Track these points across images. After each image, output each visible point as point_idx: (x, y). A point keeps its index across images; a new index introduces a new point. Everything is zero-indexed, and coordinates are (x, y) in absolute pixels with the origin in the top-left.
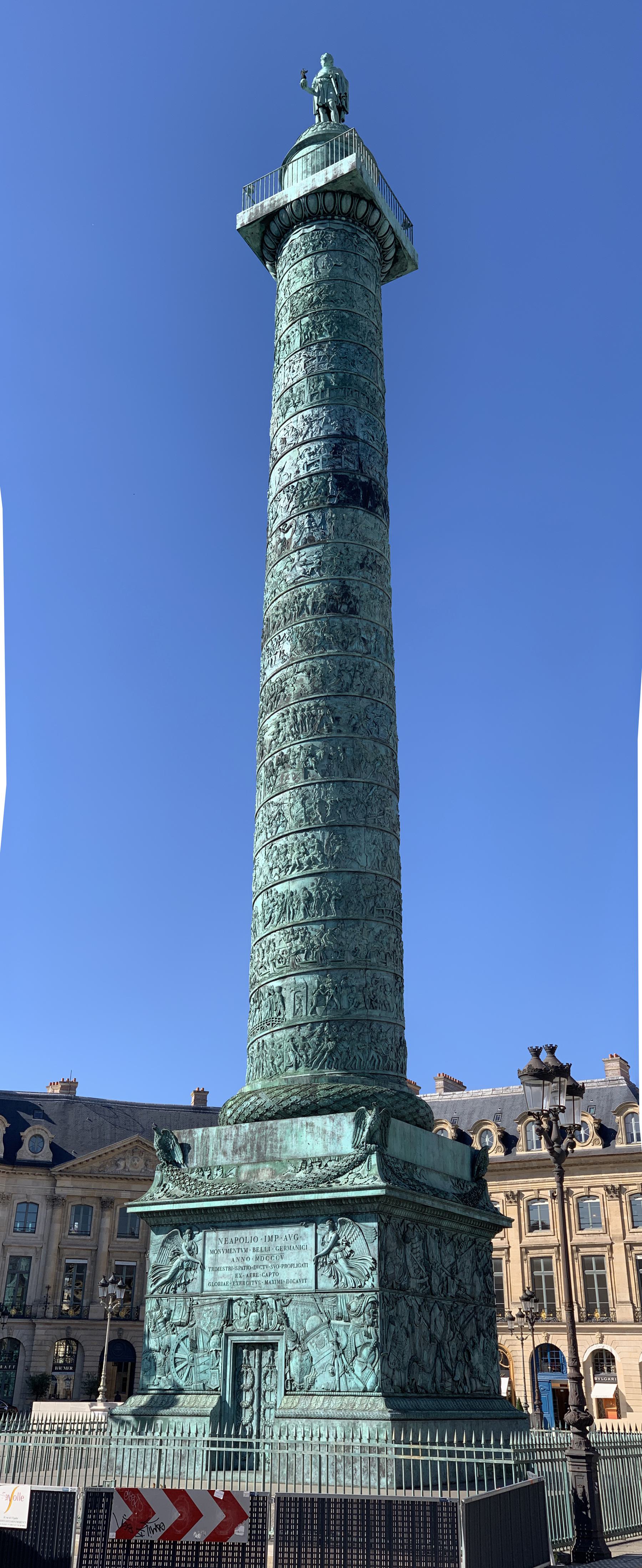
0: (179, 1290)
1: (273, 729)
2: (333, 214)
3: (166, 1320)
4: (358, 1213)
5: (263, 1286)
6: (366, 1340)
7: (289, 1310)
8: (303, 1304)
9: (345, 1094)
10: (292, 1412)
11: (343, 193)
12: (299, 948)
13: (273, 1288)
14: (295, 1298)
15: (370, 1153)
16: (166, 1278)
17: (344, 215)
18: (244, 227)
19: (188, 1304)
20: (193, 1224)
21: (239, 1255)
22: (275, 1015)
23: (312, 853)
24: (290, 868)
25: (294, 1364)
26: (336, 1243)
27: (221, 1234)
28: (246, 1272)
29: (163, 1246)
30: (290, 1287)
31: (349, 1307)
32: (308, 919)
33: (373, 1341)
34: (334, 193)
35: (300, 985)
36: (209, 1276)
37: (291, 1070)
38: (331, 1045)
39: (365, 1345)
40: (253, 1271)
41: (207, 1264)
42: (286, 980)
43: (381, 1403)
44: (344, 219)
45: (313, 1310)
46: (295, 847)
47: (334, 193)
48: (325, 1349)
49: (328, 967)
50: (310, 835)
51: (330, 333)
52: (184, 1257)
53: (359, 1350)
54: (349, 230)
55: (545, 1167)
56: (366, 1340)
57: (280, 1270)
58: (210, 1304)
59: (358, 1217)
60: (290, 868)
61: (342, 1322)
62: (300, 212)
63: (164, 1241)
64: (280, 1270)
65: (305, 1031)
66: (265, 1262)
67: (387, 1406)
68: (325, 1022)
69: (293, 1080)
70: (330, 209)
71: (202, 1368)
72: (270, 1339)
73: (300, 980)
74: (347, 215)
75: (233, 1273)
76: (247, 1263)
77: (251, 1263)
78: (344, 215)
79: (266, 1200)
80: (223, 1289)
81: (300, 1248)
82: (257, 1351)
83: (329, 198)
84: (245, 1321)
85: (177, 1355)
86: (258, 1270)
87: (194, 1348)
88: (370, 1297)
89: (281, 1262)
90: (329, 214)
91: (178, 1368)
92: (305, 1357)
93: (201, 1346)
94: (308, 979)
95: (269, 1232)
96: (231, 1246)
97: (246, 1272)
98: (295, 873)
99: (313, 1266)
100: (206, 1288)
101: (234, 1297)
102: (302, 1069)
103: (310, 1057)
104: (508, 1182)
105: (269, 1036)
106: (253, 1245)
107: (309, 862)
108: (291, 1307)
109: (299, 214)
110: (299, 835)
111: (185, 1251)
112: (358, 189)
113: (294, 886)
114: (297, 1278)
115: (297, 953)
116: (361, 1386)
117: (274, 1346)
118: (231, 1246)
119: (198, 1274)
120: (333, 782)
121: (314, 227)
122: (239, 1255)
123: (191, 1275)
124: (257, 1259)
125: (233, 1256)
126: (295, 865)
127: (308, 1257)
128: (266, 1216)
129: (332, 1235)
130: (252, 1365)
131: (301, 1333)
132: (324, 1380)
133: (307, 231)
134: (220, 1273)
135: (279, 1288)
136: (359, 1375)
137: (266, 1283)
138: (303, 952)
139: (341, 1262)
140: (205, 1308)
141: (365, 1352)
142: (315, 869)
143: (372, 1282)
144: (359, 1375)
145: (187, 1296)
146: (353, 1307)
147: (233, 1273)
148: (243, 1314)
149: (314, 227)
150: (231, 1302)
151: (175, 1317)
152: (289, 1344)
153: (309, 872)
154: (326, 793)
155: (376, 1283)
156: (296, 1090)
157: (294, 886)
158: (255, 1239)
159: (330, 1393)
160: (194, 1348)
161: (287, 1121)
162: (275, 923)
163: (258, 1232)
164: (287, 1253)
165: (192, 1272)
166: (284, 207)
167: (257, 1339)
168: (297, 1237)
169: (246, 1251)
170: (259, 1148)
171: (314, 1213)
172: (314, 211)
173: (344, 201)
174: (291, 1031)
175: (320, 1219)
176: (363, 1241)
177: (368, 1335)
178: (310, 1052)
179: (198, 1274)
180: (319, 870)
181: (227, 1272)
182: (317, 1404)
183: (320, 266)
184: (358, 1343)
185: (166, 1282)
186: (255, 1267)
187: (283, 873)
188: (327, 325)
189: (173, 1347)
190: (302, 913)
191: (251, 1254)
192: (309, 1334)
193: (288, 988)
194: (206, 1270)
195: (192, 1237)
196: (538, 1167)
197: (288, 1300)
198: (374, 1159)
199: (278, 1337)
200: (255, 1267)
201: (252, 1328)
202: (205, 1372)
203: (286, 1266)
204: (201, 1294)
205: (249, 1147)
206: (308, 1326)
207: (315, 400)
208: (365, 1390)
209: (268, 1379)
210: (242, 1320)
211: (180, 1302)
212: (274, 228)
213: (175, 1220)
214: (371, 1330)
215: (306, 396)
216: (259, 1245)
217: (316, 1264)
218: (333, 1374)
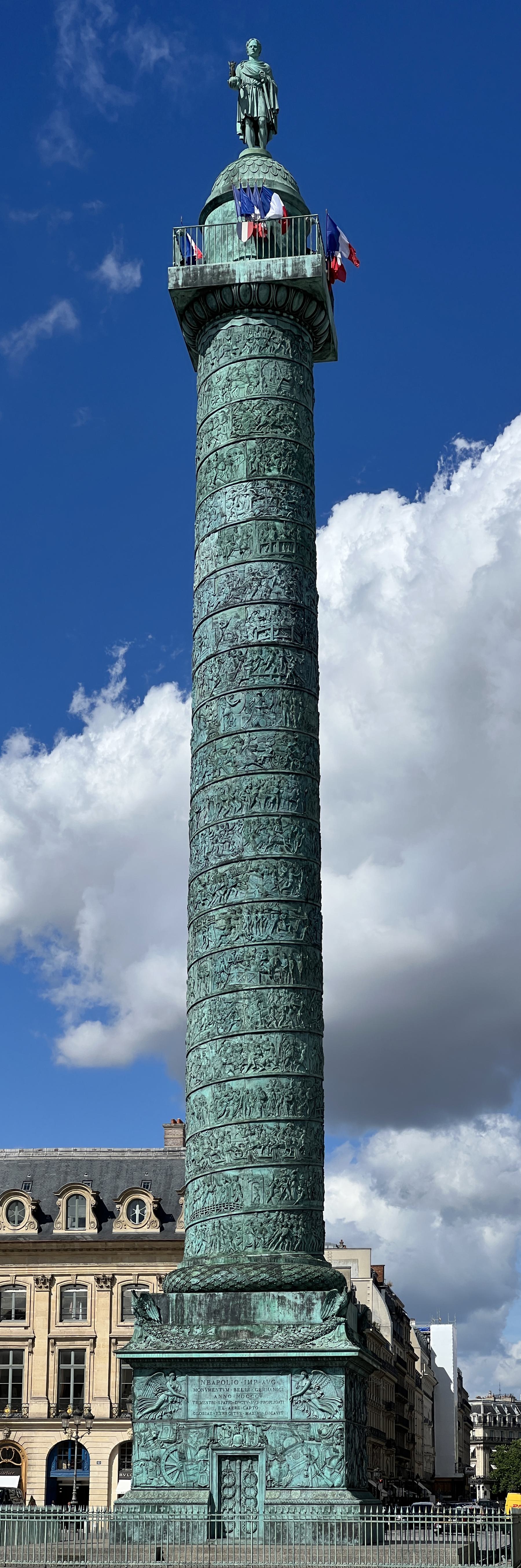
0: (165, 1417)
2: (282, 309)
3: (155, 1438)
4: (328, 1367)
5: (244, 1416)
6: (334, 1454)
7: (268, 1434)
8: (280, 1429)
9: (303, 1274)
10: (278, 1501)
11: (297, 290)
12: (257, 1143)
13: (254, 1418)
15: (340, 1323)
16: (154, 1408)
17: (293, 313)
18: (177, 289)
19: (175, 1427)
20: (176, 1369)
21: (221, 1393)
22: (232, 1200)
23: (267, 1056)
24: (246, 1068)
26: (309, 1387)
27: (203, 1378)
28: (228, 1406)
30: (268, 1417)
31: (320, 1432)
32: (263, 1118)
33: (340, 1455)
34: (288, 289)
35: (258, 1177)
36: (192, 1407)
37: (250, 1250)
38: (284, 1230)
39: (334, 1457)
40: (234, 1405)
41: (190, 1399)
42: (243, 1172)
43: (348, 1495)
44: (292, 317)
46: (251, 1048)
47: (288, 289)
48: (300, 1459)
49: (283, 1163)
50: (264, 1037)
51: (279, 469)
52: (169, 1393)
53: (328, 1461)
54: (295, 331)
55: (89, 1250)
56: (334, 1454)
57: (259, 1405)
58: (196, 1428)
59: (328, 1370)
60: (246, 1068)
61: (314, 1442)
62: (248, 298)
63: (149, 1380)
64: (259, 1405)
65: (261, 1218)
66: (246, 1399)
67: (353, 1495)
68: (279, 1211)
69: (256, 1259)
70: (280, 305)
71: (191, 1472)
72: (252, 1452)
73: (257, 1172)
74: (295, 314)
75: (216, 1406)
76: (229, 1399)
77: (232, 1399)
78: (293, 313)
79: (252, 1355)
80: (208, 1417)
81: (276, 1390)
82: (238, 1461)
83: (282, 293)
84: (230, 1440)
85: (167, 1463)
86: (239, 1404)
87: (182, 1457)
88: (338, 1426)
89: (260, 1399)
90: (278, 308)
91: (168, 1472)
92: (283, 1466)
94: (265, 1172)
95: (249, 1378)
97: (228, 1406)
98: (251, 1073)
99: (289, 1403)
101: (219, 1424)
102: (260, 1249)
103: (267, 1240)
104: (40, 1265)
105: (227, 1219)
106: (234, 1386)
107: (265, 1064)
108: (270, 1431)
109: (246, 300)
110: (254, 1036)
111: (170, 1388)
112: (314, 291)
113: (250, 1085)
114: (274, 1411)
115: (255, 1147)
116: (330, 1484)
117: (255, 1458)
120: (285, 988)
121: (261, 321)
122: (221, 1393)
123: (175, 1406)
124: (238, 1396)
125: (214, 1394)
126: (251, 1065)
128: (246, 1365)
129: (306, 1382)
130: (233, 1469)
131: (279, 1450)
133: (253, 322)
134: (204, 1406)
135: (258, 1417)
136: (329, 1476)
137: (247, 1414)
138: (260, 1147)
139: (315, 1401)
140: (192, 1431)
141: (334, 1462)
142: (269, 1071)
143: (340, 1415)
144: (329, 1476)
146: (324, 1432)
147: (216, 1406)
148: (227, 1436)
149: (261, 321)
150: (216, 1426)
151: (163, 1436)
152: (270, 1456)
153: (264, 1073)
154: (280, 997)
155: (342, 1416)
156: (264, 1269)
157: (250, 1085)
158: (236, 1382)
159: (304, 1488)
160: (182, 1457)
161: (261, 1294)
162: (230, 1116)
163: (238, 1378)
164: (264, 1393)
165: (177, 1404)
166: (230, 286)
167: (240, 1452)
169: (228, 1390)
170: (233, 1313)
171: (290, 1365)
172: (263, 302)
173: (297, 299)
175: (295, 1370)
176: (333, 1388)
177: (336, 1451)
178: (268, 1235)
179: (182, 1406)
180: (274, 1072)
181: (211, 1405)
182: (296, 1495)
183: (268, 377)
184: (328, 1456)
185: (152, 1411)
186: (236, 1402)
187: (237, 1071)
188: (276, 457)
189: (165, 1457)
190: (258, 1111)
191: (233, 1393)
192: (286, 1450)
193: (245, 1178)
194: (190, 1403)
195: (175, 1379)
196: (81, 1250)
197: (268, 1426)
198: (342, 1328)
199: (258, 1452)
200: (236, 1402)
201: (238, 1445)
202: (194, 1475)
203: (265, 1402)
205: (223, 1312)
206: (286, 1445)
207: (264, 552)
208: (333, 1486)
209: (248, 1480)
210: (227, 1440)
212: (212, 302)
213: (159, 1365)
214: (338, 1447)
215: (255, 545)
216: (239, 1386)
217: (292, 1402)
218: (307, 1476)
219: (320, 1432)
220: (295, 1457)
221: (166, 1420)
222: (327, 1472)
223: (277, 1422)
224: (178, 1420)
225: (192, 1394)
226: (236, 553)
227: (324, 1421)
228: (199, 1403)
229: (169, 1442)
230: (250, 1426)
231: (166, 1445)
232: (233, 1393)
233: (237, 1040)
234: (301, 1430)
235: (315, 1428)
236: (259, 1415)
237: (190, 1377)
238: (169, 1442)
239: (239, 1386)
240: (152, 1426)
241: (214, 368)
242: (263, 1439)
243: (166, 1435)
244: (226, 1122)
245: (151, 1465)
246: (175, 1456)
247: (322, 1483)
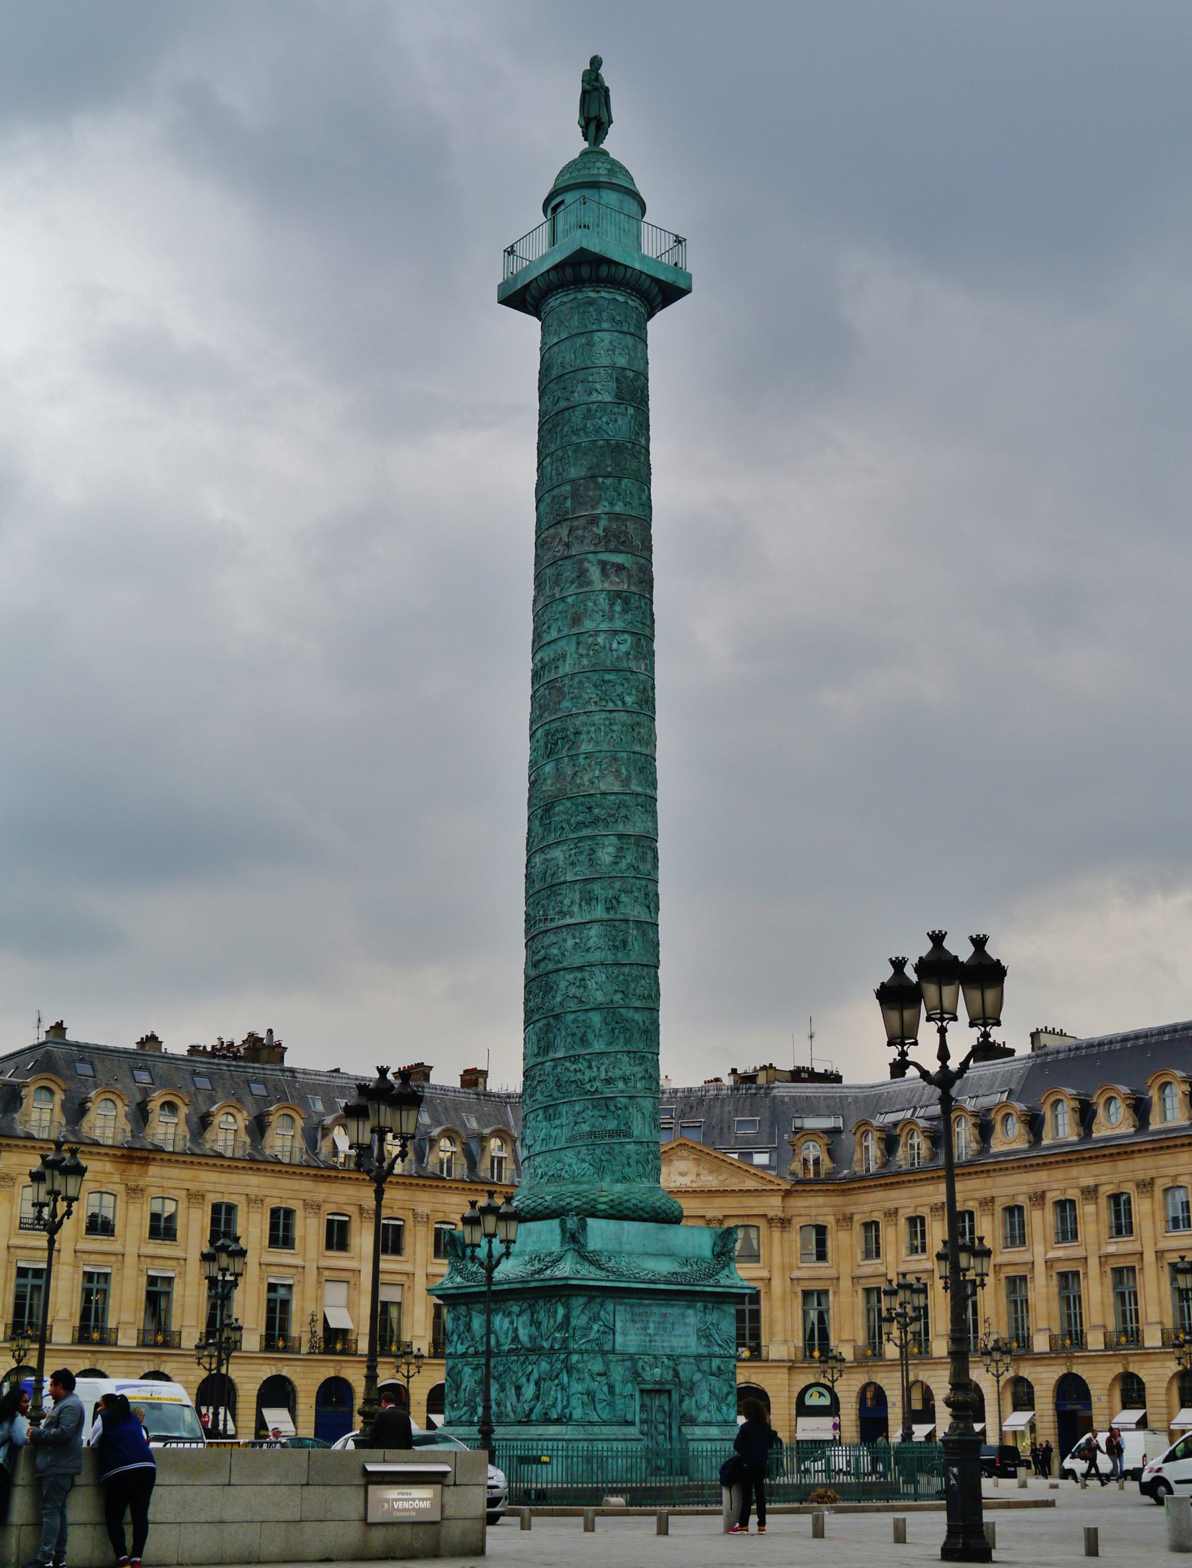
1: (611, 850)
7: (679, 1368)
13: (668, 1351)
14: (684, 1359)
21: (643, 1325)
25: (685, 1404)
28: (648, 1338)
29: (582, 1312)
30: (679, 1351)
31: (719, 1368)
36: (619, 1339)
45: (695, 1368)
71: (621, 1407)
72: (667, 1387)
80: (632, 1350)
81: (685, 1324)
87: (611, 1389)
93: (617, 1391)
95: (664, 1310)
96: (636, 1318)
97: (648, 1338)
98: (638, 1004)
100: (617, 1347)
106: (652, 1319)
118: (636, 1318)
119: (611, 1337)
122: (643, 1325)
125: (638, 1325)
127: (691, 1331)
132: (703, 1416)
134: (628, 1338)
145: (604, 1353)
159: (708, 1424)
160: (611, 1389)
164: (676, 1326)
167: (657, 1387)
168: (683, 1316)
174: (639, 1147)
181: (633, 1337)
204: (613, 1352)
211: (599, 1358)
219: (719, 1368)
220: (701, 1393)
221: (598, 1352)
222: (724, 1408)
223: (686, 1356)
224: (608, 1352)
225: (618, 1325)
226: (620, 504)
227: (721, 1356)
228: (624, 1334)
229: (600, 1375)
230: (666, 1361)
231: (598, 1378)
232: (651, 1325)
233: (626, 970)
234: (704, 1365)
235: (716, 1362)
236: (672, 1348)
237: (618, 1307)
238: (600, 1375)
239: (656, 1318)
240: (585, 1355)
241: (594, 327)
242: (676, 1374)
243: (597, 1366)
244: (617, 1049)
245: (585, 1398)
246: (605, 1389)
247: (720, 1418)
